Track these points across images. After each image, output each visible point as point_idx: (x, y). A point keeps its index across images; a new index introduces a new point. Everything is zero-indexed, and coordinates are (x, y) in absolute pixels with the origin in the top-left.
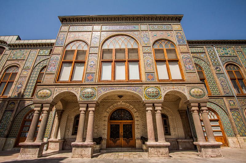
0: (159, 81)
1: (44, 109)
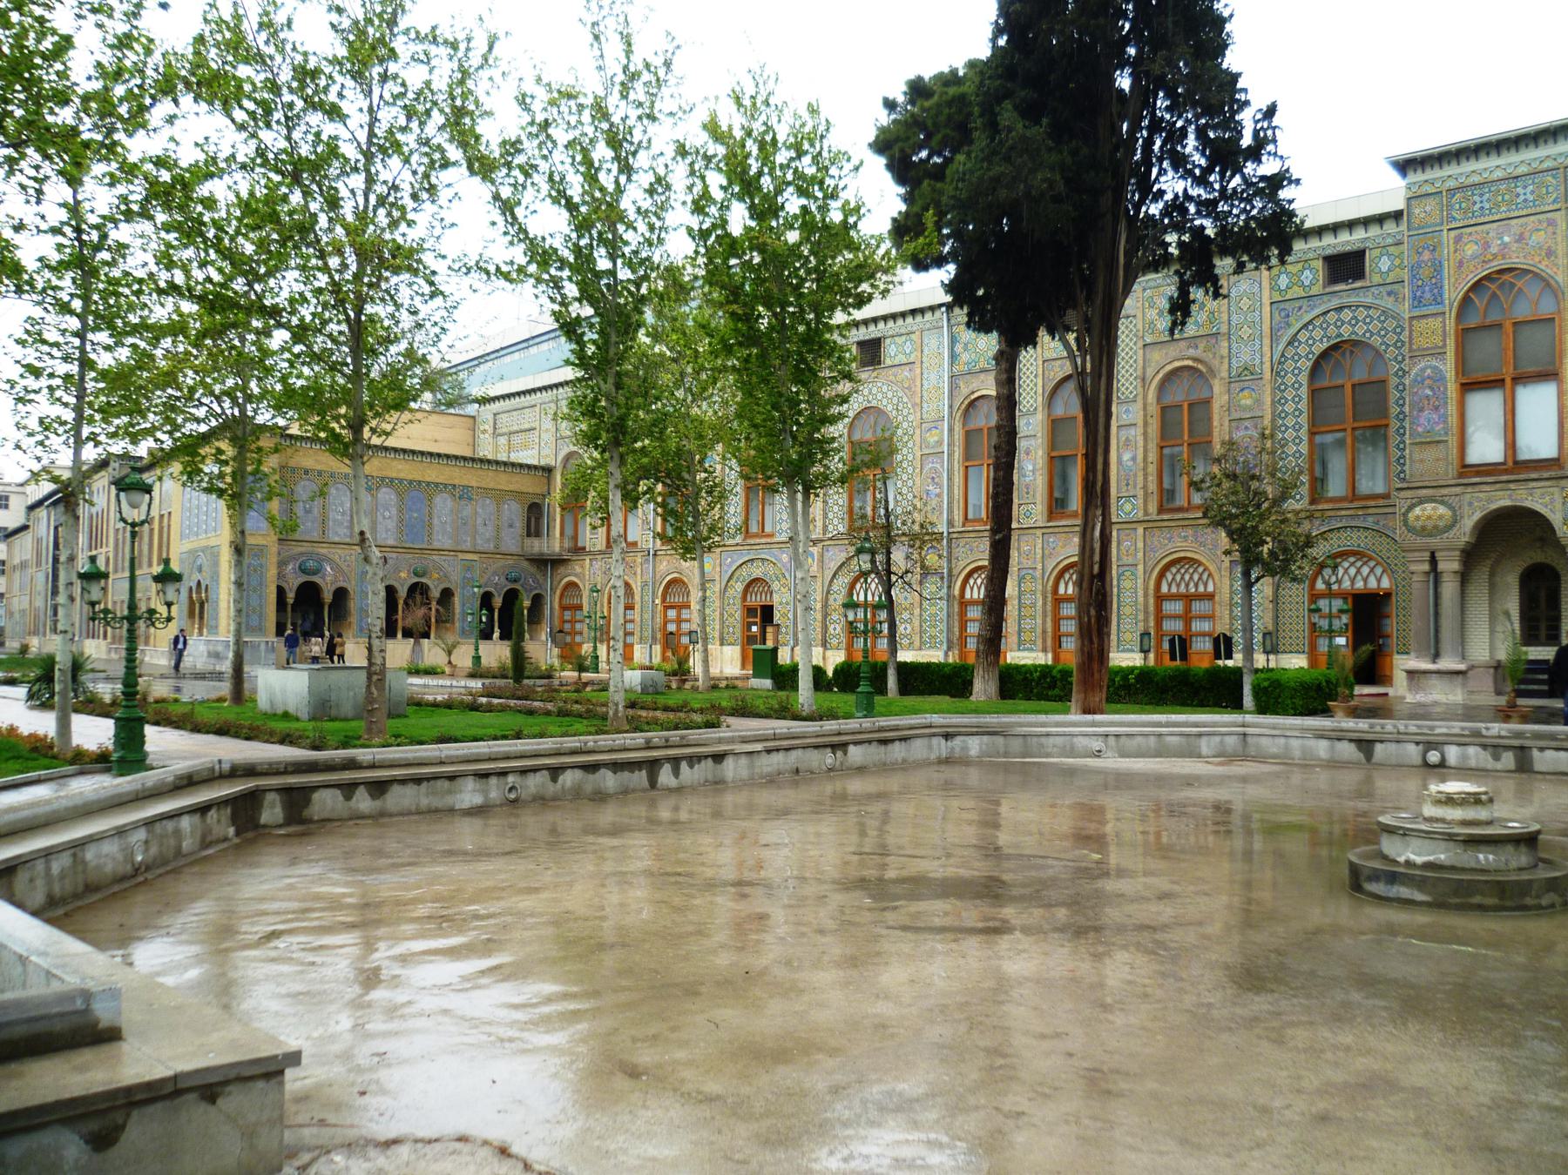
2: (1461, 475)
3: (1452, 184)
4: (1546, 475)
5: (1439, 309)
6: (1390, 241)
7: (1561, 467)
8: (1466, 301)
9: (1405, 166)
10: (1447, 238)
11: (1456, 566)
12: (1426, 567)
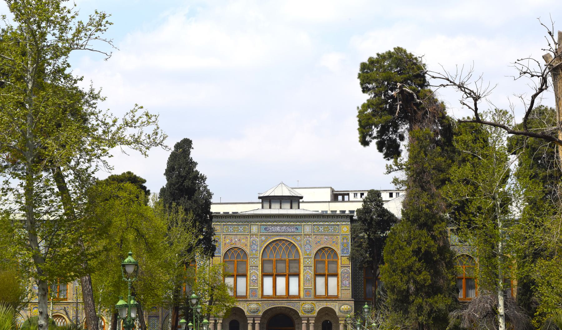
5: (219, 255)
10: (222, 237)
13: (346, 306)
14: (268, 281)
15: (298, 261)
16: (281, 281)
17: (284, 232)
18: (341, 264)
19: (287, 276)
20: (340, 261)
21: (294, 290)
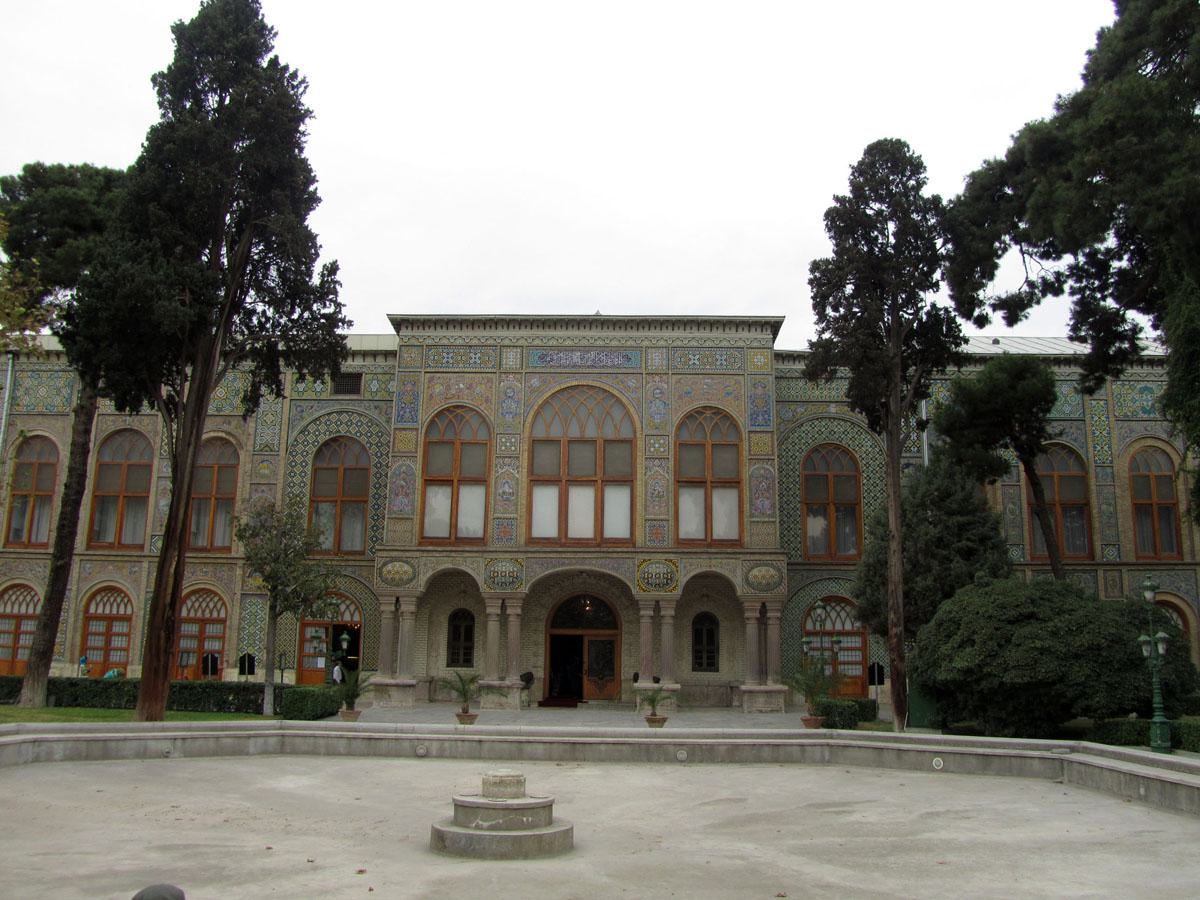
0: (678, 543)
1: (404, 608)
2: (420, 544)
3: (429, 342)
4: (475, 549)
5: (415, 426)
6: (379, 370)
7: (485, 545)
8: (432, 422)
9: (399, 323)
10: (424, 378)
11: (413, 608)
12: (393, 608)
13: (764, 569)
14: (546, 501)
15: (630, 442)
16: (582, 500)
17: (593, 366)
18: (750, 454)
19: (601, 481)
20: (745, 445)
21: (617, 525)
